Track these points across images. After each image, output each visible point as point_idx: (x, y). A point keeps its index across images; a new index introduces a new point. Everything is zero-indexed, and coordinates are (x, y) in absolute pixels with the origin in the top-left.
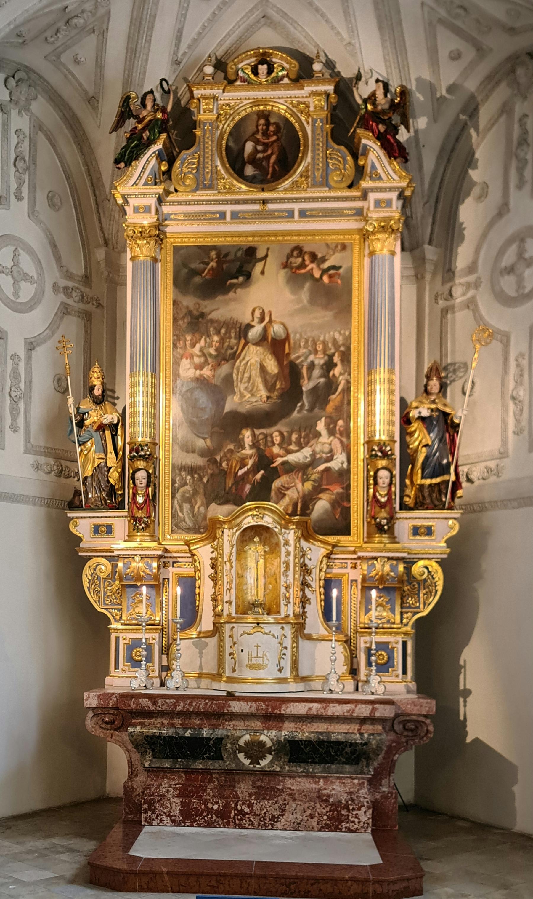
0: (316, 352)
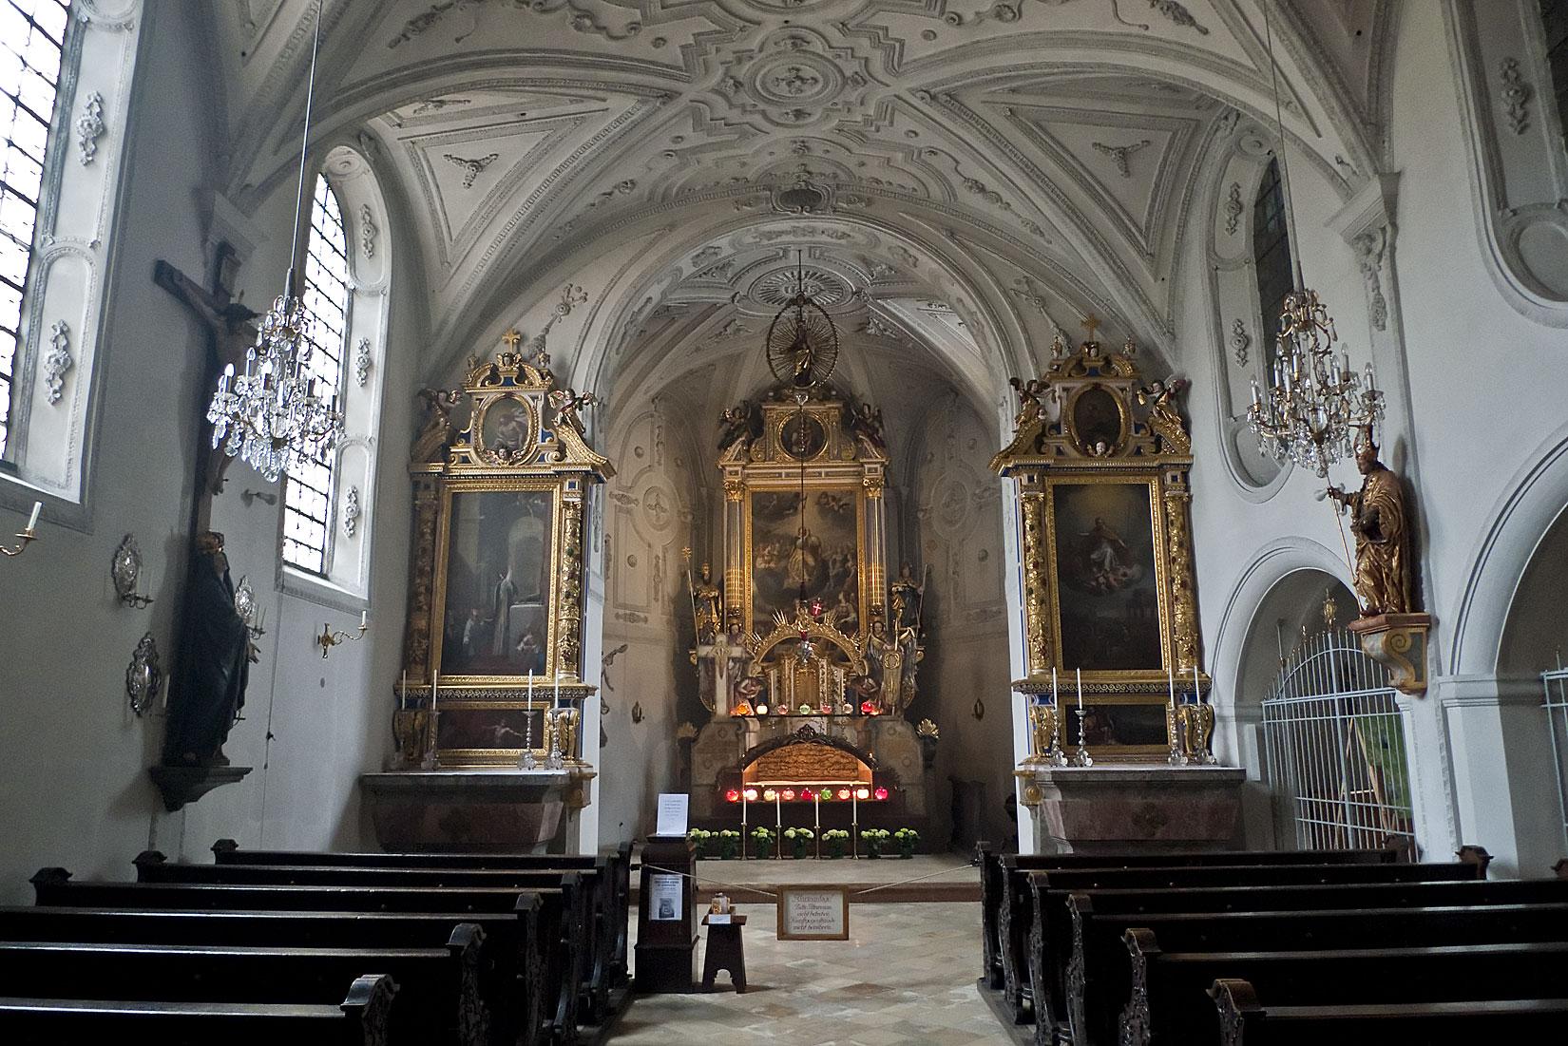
0: (837, 553)
